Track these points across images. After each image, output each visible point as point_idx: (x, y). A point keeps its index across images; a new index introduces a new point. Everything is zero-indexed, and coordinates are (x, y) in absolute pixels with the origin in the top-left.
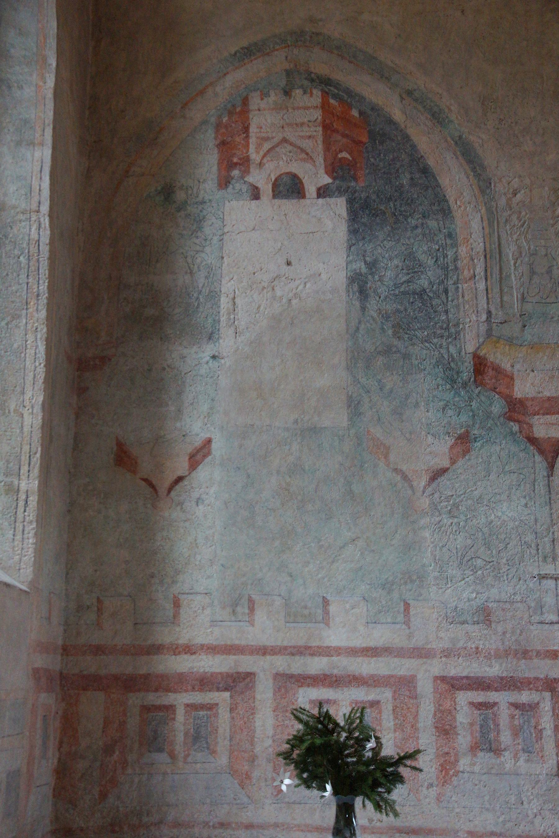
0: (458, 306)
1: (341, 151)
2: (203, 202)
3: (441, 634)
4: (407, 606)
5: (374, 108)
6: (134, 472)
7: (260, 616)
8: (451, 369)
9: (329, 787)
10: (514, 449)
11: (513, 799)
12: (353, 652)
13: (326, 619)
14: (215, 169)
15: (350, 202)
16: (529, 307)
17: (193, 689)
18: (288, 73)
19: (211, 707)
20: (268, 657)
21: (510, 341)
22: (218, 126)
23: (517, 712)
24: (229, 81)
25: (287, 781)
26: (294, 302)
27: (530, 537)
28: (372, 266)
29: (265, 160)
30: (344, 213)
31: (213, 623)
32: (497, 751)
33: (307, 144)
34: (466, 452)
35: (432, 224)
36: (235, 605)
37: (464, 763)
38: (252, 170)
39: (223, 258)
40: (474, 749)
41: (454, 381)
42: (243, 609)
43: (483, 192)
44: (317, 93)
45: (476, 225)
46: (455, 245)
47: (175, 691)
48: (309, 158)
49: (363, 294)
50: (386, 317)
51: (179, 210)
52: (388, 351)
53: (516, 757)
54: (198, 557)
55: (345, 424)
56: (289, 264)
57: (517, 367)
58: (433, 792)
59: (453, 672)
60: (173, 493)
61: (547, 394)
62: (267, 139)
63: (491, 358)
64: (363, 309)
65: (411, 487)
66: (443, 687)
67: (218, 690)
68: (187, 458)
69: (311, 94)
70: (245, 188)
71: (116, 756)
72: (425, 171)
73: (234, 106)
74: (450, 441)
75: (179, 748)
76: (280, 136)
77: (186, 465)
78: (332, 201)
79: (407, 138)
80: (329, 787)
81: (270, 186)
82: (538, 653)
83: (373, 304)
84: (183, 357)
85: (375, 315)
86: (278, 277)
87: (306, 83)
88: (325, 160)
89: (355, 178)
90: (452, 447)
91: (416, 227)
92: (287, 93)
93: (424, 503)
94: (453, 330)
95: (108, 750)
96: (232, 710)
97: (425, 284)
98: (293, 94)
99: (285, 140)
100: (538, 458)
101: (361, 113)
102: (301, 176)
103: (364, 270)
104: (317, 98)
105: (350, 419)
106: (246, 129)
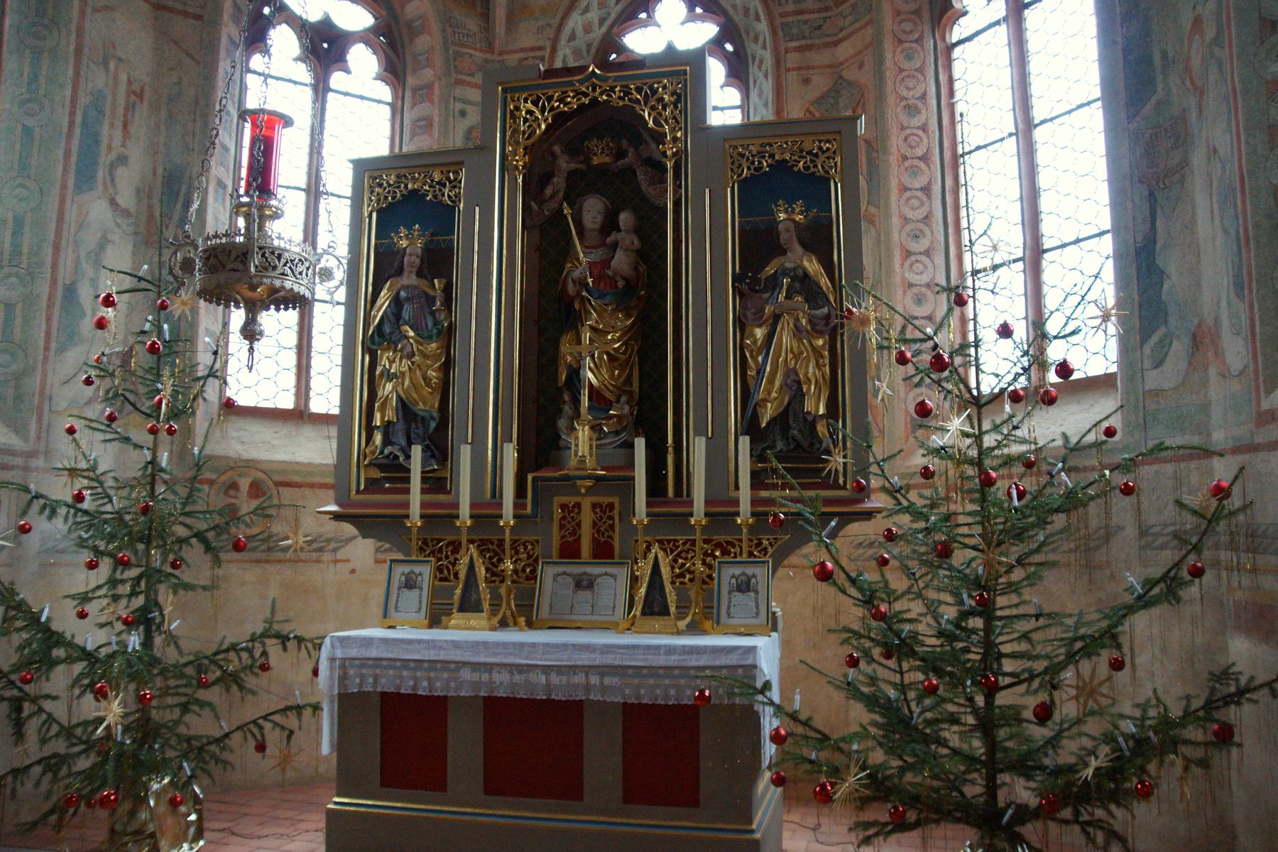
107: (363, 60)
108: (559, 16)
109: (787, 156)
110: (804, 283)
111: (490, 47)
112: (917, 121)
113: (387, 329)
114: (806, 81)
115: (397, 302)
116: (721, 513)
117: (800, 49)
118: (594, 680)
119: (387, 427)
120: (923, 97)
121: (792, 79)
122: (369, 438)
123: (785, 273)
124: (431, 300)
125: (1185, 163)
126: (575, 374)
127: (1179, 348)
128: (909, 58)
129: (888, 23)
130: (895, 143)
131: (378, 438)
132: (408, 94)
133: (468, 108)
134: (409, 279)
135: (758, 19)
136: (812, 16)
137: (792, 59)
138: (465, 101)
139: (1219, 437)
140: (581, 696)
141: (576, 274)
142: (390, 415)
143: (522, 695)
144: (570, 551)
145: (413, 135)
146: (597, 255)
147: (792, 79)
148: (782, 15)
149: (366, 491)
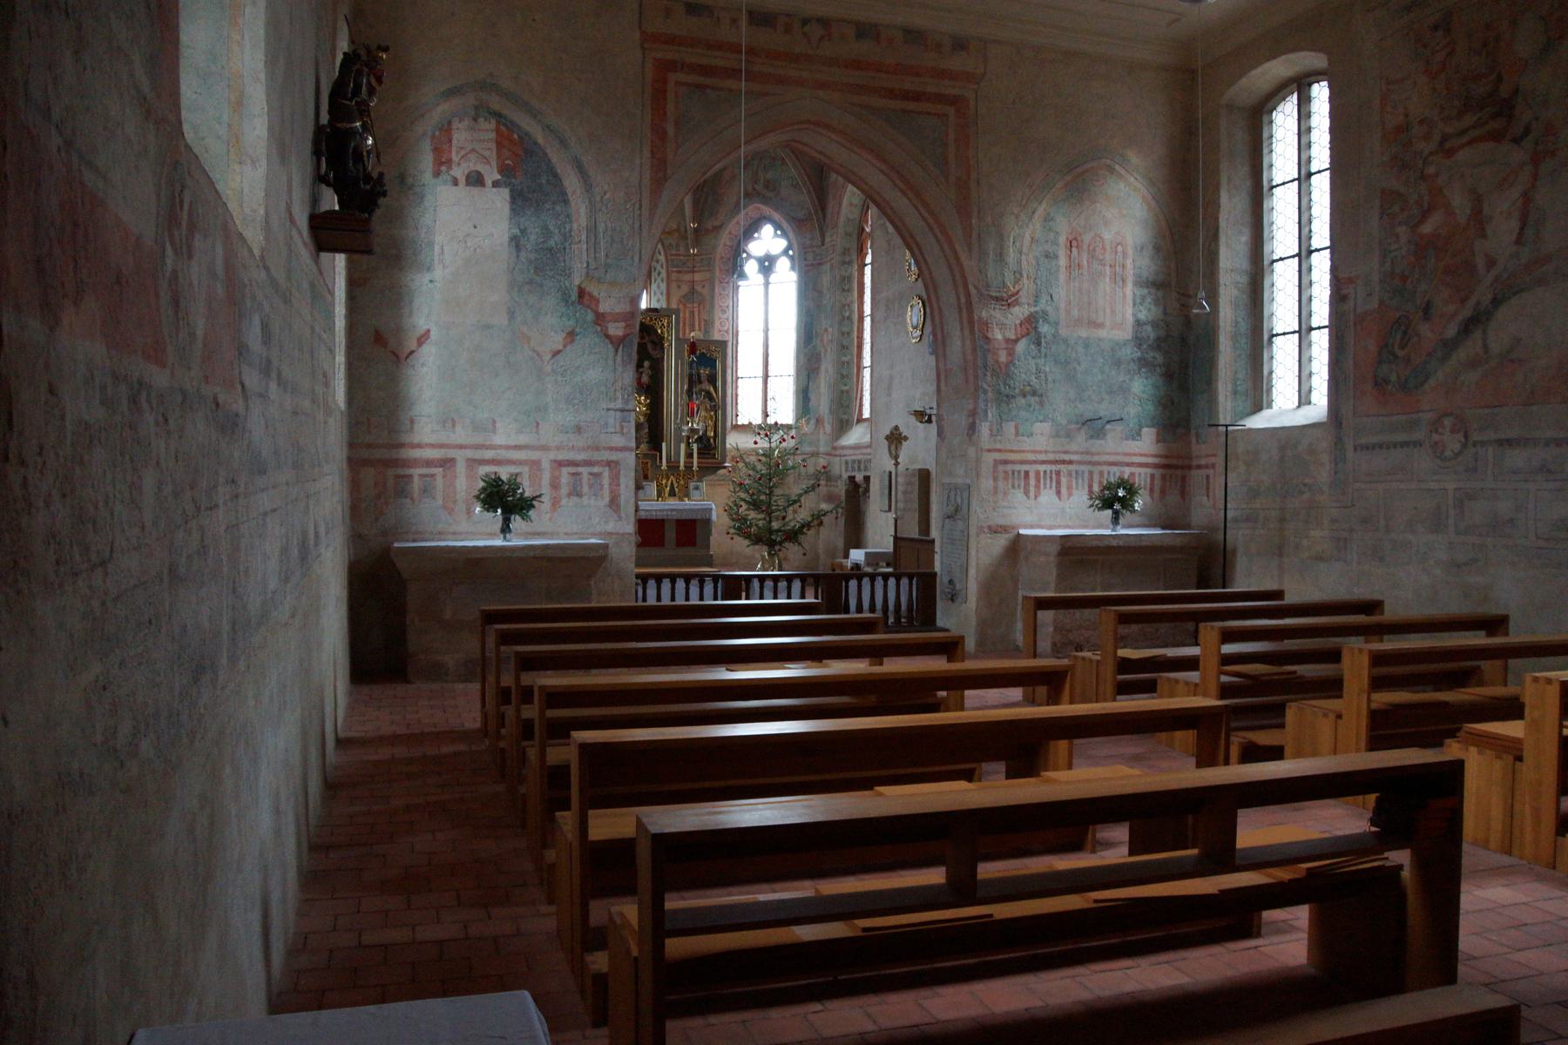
0: (571, 258)
1: (507, 159)
2: (424, 185)
3: (555, 439)
4: (538, 424)
5: (527, 134)
6: (386, 348)
7: (458, 428)
8: (565, 294)
9: (499, 511)
10: (597, 340)
11: (587, 517)
12: (508, 448)
13: (494, 430)
14: (431, 165)
15: (511, 191)
16: (609, 261)
17: (423, 466)
18: (476, 108)
19: (433, 476)
20: (463, 450)
21: (599, 280)
22: (433, 137)
23: (591, 477)
24: (440, 109)
25: (478, 509)
26: (478, 250)
27: (603, 389)
29: (461, 162)
30: (508, 198)
31: (433, 432)
32: (580, 495)
33: (487, 153)
34: (572, 341)
35: (558, 208)
36: (445, 422)
37: (564, 502)
38: (453, 167)
39: (435, 221)
40: (569, 495)
41: (567, 302)
42: (449, 425)
43: (587, 191)
44: (493, 122)
45: (583, 211)
46: (571, 222)
47: (412, 468)
48: (488, 163)
49: (518, 247)
50: (530, 262)
51: (409, 189)
52: (531, 282)
53: (589, 498)
54: (424, 396)
55: (506, 322)
56: (475, 227)
57: (602, 294)
58: (548, 515)
59: (560, 457)
60: (408, 360)
61: (617, 311)
62: (462, 148)
63: (588, 289)
64: (518, 256)
65: (542, 360)
66: (556, 465)
67: (436, 467)
68: (416, 341)
69: (490, 122)
70: (449, 178)
71: (382, 500)
72: (555, 175)
73: (443, 126)
75: (416, 495)
76: (470, 148)
77: (415, 344)
78: (501, 190)
79: (545, 154)
80: (499, 511)
81: (464, 178)
82: (604, 448)
83: (523, 254)
84: (412, 280)
85: (524, 260)
86: (468, 235)
87: (486, 114)
88: (497, 164)
89: (515, 178)
90: (566, 338)
91: (549, 210)
92: (475, 120)
93: (548, 368)
94: (567, 272)
95: (379, 496)
96: (443, 477)
97: (554, 245)
98: (479, 121)
99: (473, 150)
100: (610, 346)
101: (519, 137)
102: (483, 173)
103: (519, 234)
104: (493, 125)
105: (509, 320)
106: (450, 141)
109: (704, 351)
110: (709, 395)
112: (725, 316)
114: (679, 287)
116: (689, 467)
117: (679, 272)
118: (669, 513)
120: (728, 307)
121: (674, 285)
123: (704, 390)
125: (819, 368)
127: (813, 422)
128: (724, 289)
129: (717, 273)
130: (717, 324)
135: (660, 253)
136: (682, 258)
137: (674, 276)
139: (822, 450)
140: (665, 518)
143: (649, 518)
147: (674, 285)
148: (672, 255)
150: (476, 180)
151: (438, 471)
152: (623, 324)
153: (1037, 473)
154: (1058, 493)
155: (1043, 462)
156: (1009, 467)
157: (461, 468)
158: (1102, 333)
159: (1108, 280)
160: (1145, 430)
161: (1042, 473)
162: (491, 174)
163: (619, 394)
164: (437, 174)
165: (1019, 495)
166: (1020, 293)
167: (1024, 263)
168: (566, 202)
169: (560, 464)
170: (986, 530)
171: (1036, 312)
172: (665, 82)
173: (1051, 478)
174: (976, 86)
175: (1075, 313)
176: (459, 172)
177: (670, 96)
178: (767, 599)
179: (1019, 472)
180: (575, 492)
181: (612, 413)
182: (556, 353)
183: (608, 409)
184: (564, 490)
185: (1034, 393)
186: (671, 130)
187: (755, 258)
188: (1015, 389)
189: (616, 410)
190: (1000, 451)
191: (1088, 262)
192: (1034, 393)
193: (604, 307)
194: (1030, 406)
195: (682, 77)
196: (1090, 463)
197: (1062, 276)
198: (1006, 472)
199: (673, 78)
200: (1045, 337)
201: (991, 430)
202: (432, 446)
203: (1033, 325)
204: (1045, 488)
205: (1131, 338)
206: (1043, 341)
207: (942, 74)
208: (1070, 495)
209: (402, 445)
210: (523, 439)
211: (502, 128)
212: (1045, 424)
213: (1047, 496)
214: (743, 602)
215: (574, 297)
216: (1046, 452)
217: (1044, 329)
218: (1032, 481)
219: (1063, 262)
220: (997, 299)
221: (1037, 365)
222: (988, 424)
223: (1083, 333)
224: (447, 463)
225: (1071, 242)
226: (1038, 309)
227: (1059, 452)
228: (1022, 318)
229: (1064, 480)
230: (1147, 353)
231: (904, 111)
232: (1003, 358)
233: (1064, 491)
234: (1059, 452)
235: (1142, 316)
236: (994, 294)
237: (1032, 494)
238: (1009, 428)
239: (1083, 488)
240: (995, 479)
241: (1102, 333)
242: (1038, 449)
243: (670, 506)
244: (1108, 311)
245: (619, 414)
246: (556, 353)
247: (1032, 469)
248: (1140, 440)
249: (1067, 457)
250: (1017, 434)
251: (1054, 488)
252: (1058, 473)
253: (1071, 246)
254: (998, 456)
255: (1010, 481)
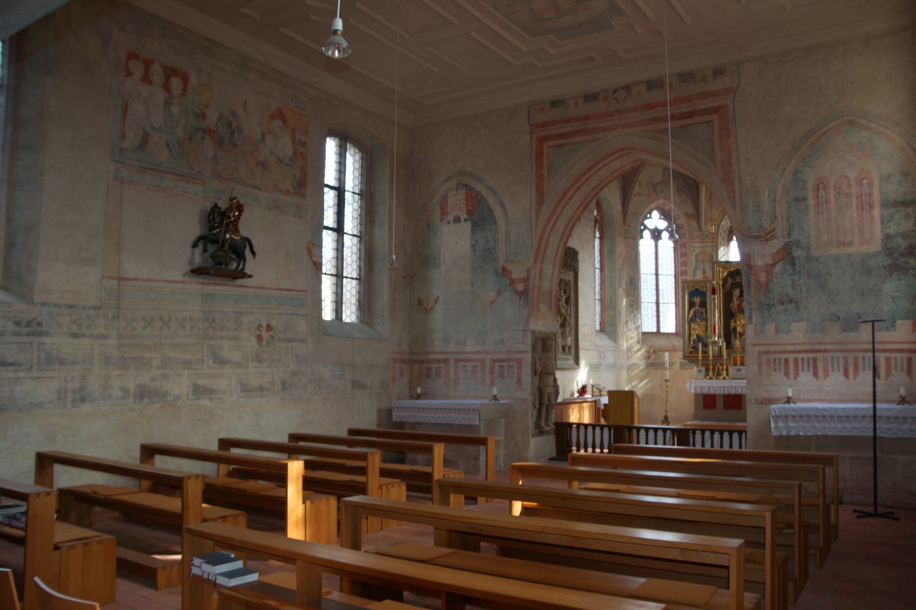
12: (471, 353)
15: (472, 222)
19: (440, 368)
28: (477, 242)
44: (464, 189)
62: (451, 206)
64: (475, 255)
72: (491, 211)
74: (495, 293)
92: (457, 190)
99: (456, 205)
101: (475, 194)
104: (464, 191)
106: (447, 204)
107: (665, 235)
108: (719, 221)
111: (700, 230)
113: (693, 319)
115: (695, 313)
119: (694, 340)
122: (690, 342)
124: (702, 313)
126: (735, 329)
131: (692, 342)
132: (679, 246)
133: (696, 249)
134: (697, 308)
138: (694, 247)
141: (734, 307)
142: (695, 337)
144: (735, 364)
145: (681, 257)
146: (739, 302)
149: (690, 353)
150: (457, 220)
151: (442, 365)
152: (523, 284)
153: (796, 360)
154: (816, 374)
155: (800, 352)
156: (771, 357)
157: (452, 363)
158: (851, 250)
159: (854, 207)
160: (899, 322)
161: (800, 361)
162: (464, 216)
163: (522, 322)
164: (442, 220)
165: (780, 376)
166: (776, 230)
167: (778, 208)
168: (496, 223)
169: (494, 361)
170: (753, 402)
171: (790, 242)
172: (542, 148)
173: (808, 363)
174: (733, 96)
175: (825, 238)
176: (450, 218)
177: (545, 155)
178: (651, 444)
179: (780, 360)
180: (501, 376)
181: (518, 332)
182: (492, 303)
183: (516, 331)
184: (496, 375)
185: (791, 301)
186: (545, 173)
187: (650, 230)
188: (774, 299)
189: (521, 330)
190: (763, 344)
191: (835, 198)
192: (791, 301)
193: (515, 276)
194: (787, 310)
195: (550, 143)
196: (844, 351)
197: (812, 213)
198: (768, 360)
199: (546, 144)
200: (799, 259)
201: (756, 330)
202: (441, 353)
203: (788, 251)
204: (803, 369)
205: (880, 249)
206: (797, 262)
207: (707, 95)
208: (826, 375)
209: (428, 353)
210: (478, 348)
211: (468, 192)
212: (801, 324)
213: (805, 377)
214: (627, 445)
215: (500, 270)
216: (803, 344)
217: (797, 253)
218: (791, 366)
219: (811, 202)
220: (757, 237)
221: (793, 281)
222: (753, 326)
223: (834, 251)
224: (446, 361)
225: (818, 185)
226: (791, 239)
227: (815, 344)
228: (778, 248)
229: (820, 366)
230: (898, 260)
231: (682, 126)
232: (763, 277)
233: (821, 372)
234: (815, 344)
235: (891, 231)
236: (754, 234)
237: (792, 376)
238: (770, 328)
239: (839, 370)
240: (760, 365)
241: (851, 250)
242: (795, 342)
243: (719, 386)
244: (856, 231)
245: (522, 333)
246: (492, 303)
247: (791, 357)
248: (895, 330)
249: (823, 347)
250: (777, 331)
251: (811, 371)
252: (815, 360)
253: (818, 189)
254: (762, 348)
255: (772, 366)
